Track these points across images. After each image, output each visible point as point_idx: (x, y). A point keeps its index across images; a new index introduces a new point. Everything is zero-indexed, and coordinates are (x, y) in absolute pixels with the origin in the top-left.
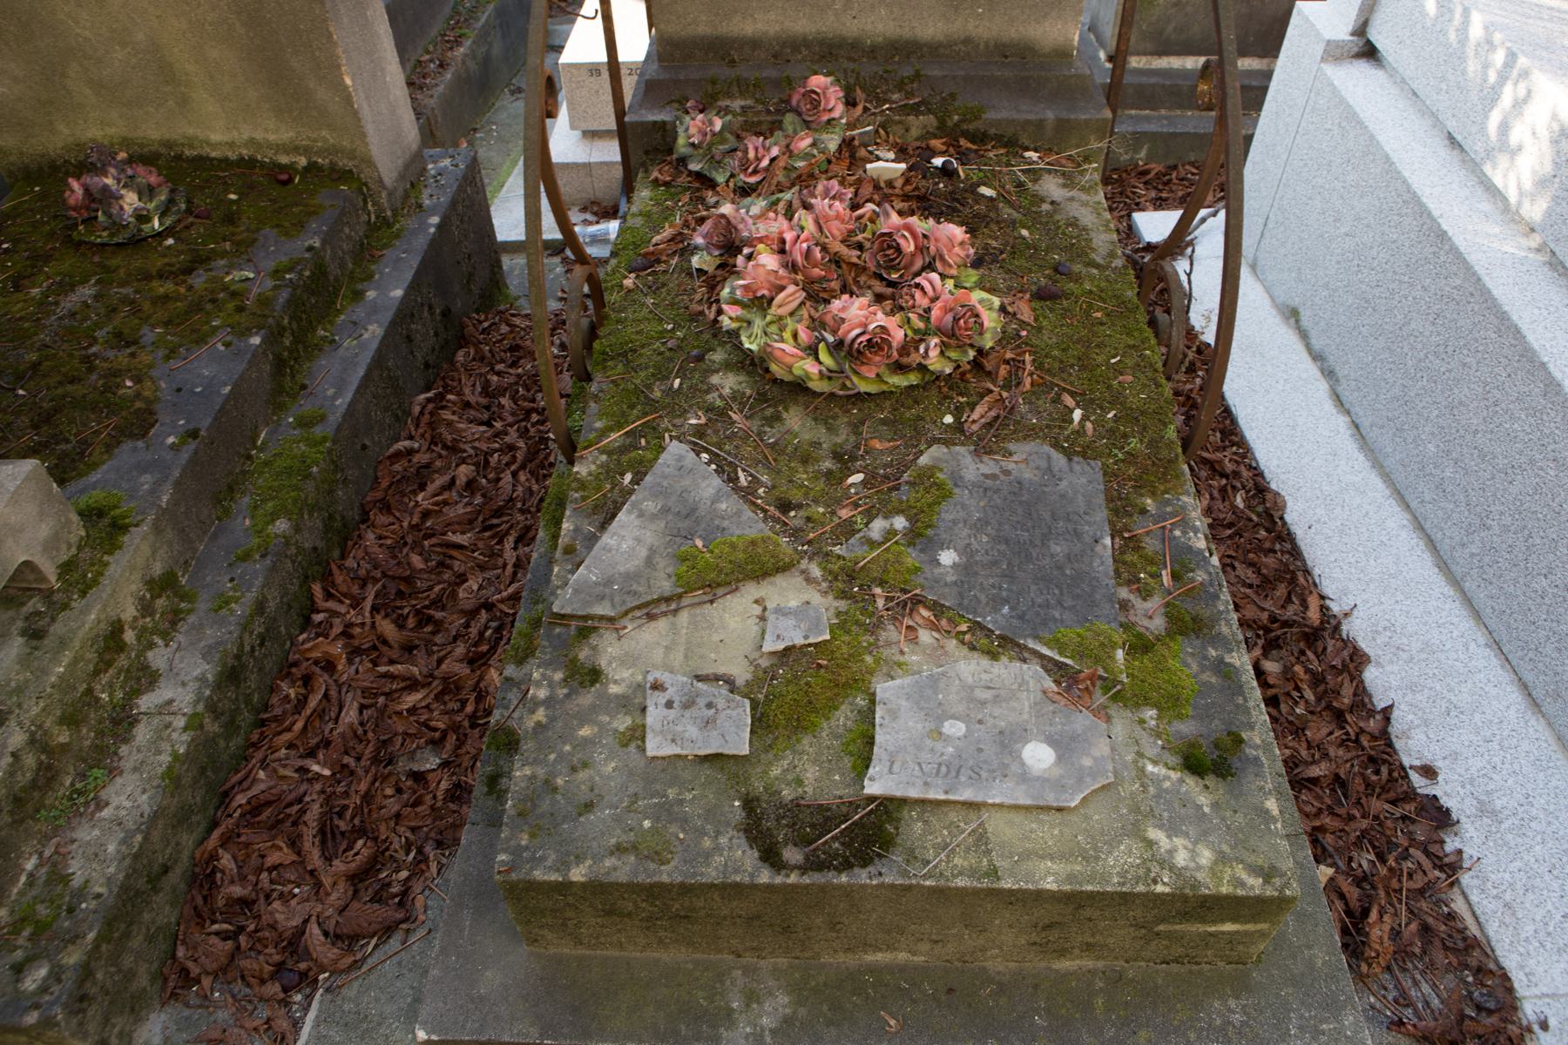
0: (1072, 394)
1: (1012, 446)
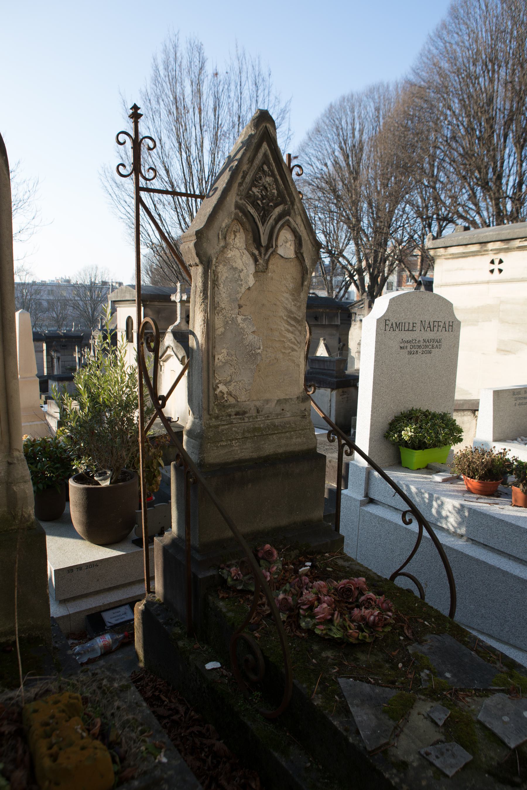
1: (424, 638)
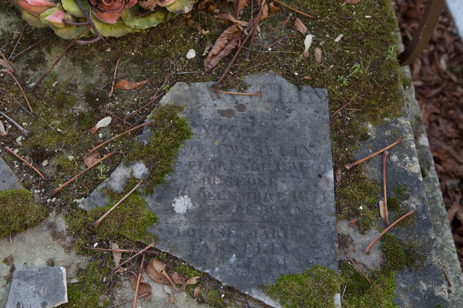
0: (305, 20)
1: (247, 79)
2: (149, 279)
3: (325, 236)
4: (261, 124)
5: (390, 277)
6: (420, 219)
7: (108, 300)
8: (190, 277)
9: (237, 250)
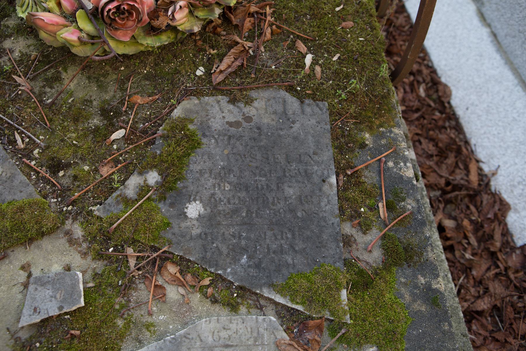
0: (305, 41)
1: (254, 94)
2: (163, 281)
3: (330, 236)
4: (267, 134)
5: (391, 272)
6: (416, 219)
7: (124, 302)
8: (203, 278)
9: (248, 251)
